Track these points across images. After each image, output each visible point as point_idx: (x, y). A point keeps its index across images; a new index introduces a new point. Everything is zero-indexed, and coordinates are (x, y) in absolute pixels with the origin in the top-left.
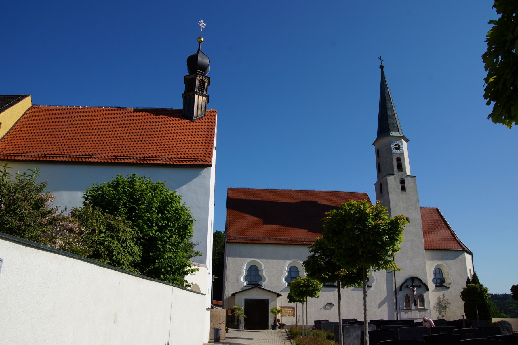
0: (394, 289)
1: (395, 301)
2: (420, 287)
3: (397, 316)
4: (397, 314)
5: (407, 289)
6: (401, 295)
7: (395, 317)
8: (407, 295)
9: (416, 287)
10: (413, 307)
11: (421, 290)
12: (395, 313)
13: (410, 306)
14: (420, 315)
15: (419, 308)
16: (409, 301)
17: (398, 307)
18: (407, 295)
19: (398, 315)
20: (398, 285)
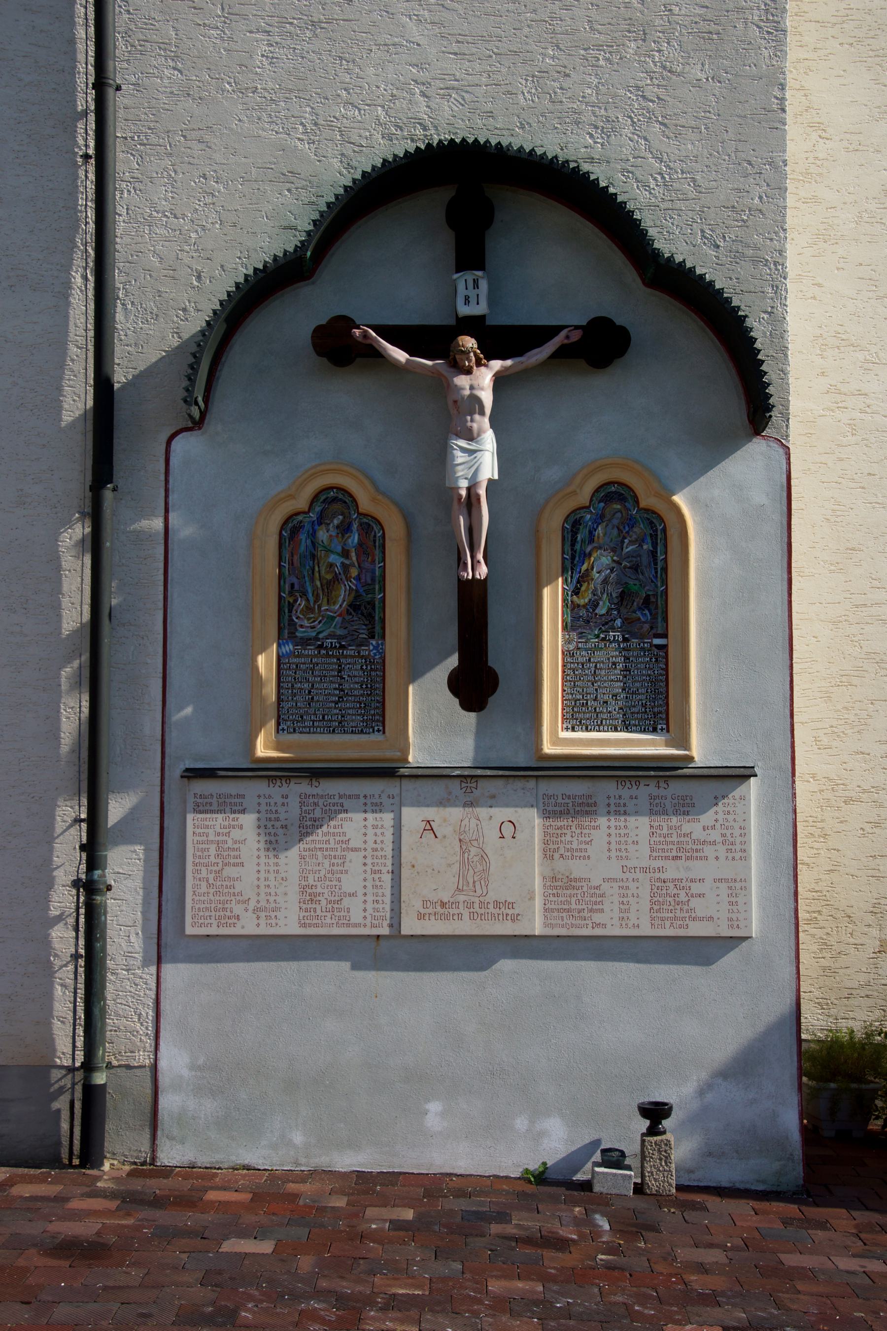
0: (77, 399)
1: (74, 613)
2: (600, 346)
3: (90, 889)
4: (92, 850)
5: (345, 395)
6: (214, 499)
7: (64, 899)
8: (333, 501)
9: (498, 341)
10: (430, 724)
11: (604, 426)
12: (69, 811)
13: (375, 709)
14: (558, 884)
15: (558, 738)
16: (367, 612)
17: (135, 722)
18: (333, 501)
19: (127, 869)
20: (158, 323)
